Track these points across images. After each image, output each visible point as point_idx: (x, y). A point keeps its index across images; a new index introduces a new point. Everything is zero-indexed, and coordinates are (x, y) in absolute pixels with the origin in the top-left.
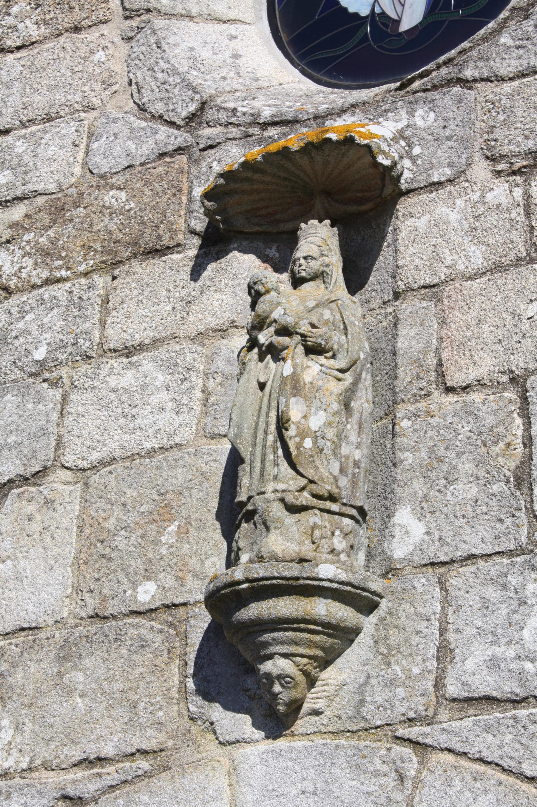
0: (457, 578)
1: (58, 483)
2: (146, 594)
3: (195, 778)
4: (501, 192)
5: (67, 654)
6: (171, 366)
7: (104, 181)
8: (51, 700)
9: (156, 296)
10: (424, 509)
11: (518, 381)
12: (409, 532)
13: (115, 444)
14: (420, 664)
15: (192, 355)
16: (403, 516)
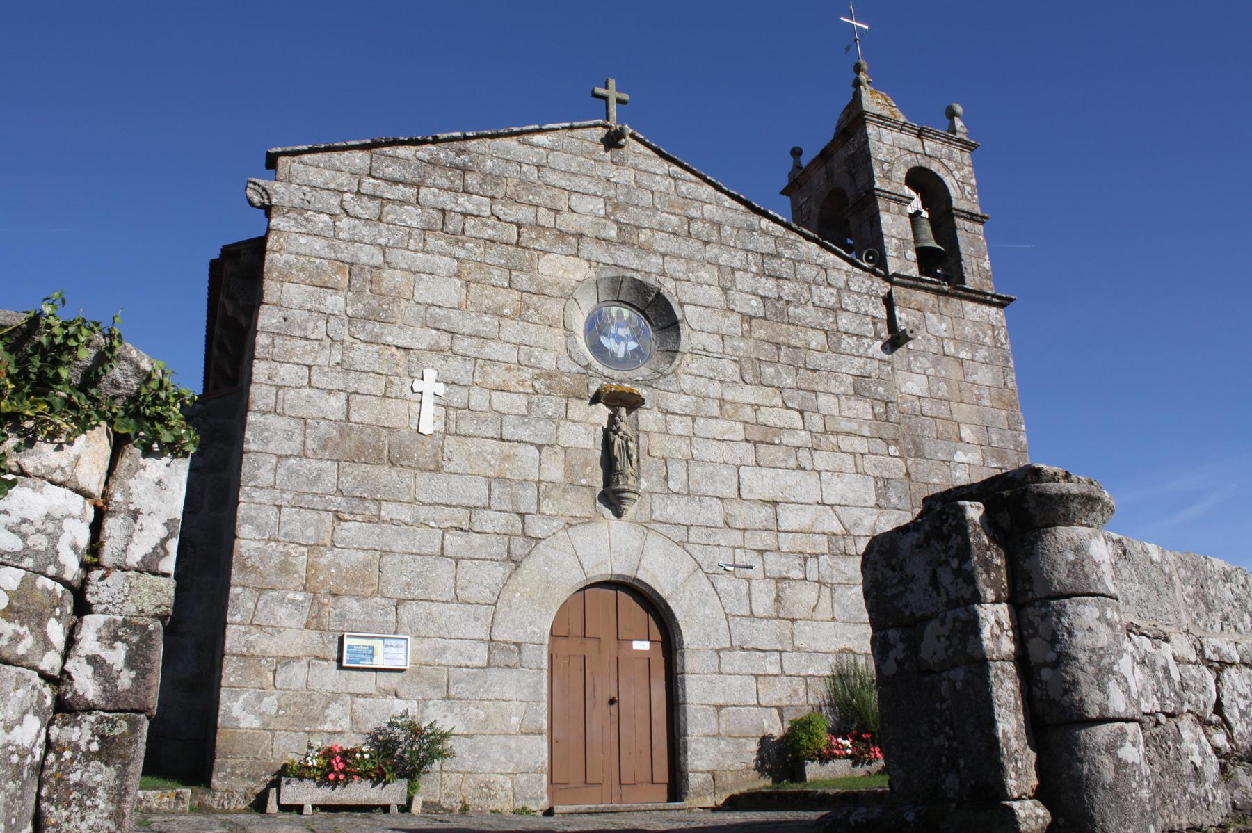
0: (654, 496)
1: (557, 449)
2: (584, 482)
3: (600, 525)
4: (660, 415)
5: (565, 491)
6: (586, 429)
7: (563, 373)
8: (562, 501)
9: (580, 409)
10: (647, 480)
11: (665, 459)
12: (644, 484)
13: (572, 444)
14: (648, 512)
15: (591, 428)
16: (642, 480)
